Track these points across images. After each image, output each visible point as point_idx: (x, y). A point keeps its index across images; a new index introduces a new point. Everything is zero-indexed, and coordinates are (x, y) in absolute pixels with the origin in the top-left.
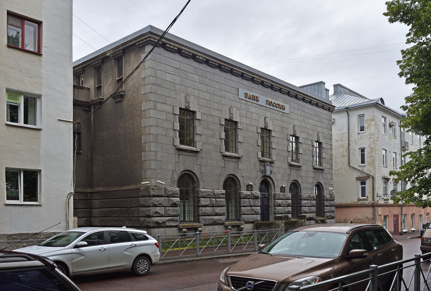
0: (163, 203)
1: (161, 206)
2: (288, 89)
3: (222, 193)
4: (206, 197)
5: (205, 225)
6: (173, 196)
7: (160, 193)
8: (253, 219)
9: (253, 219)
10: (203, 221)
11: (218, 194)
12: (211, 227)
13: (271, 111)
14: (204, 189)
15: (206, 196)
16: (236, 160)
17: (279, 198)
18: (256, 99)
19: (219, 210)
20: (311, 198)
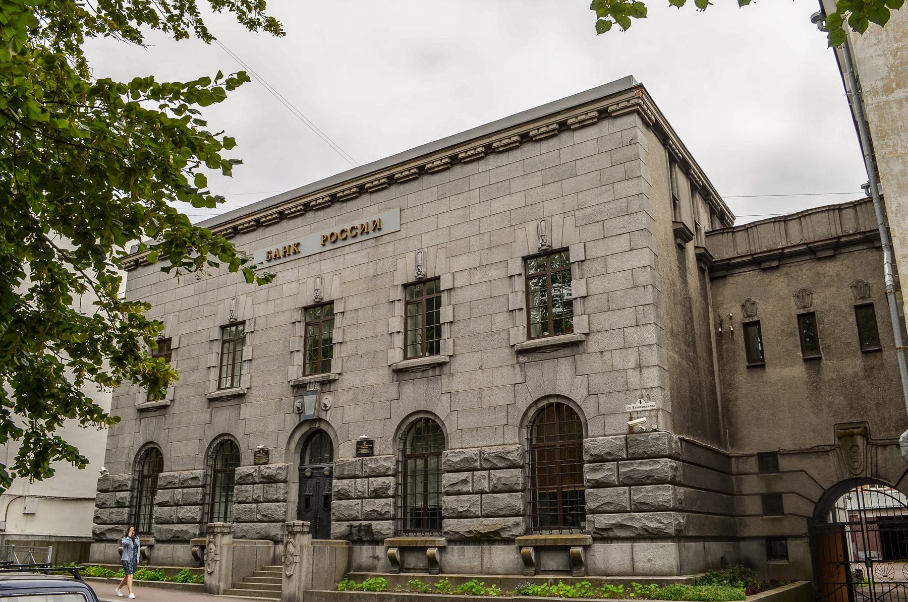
0: (107, 501)
1: (106, 506)
2: (382, 175)
3: (194, 476)
4: (167, 487)
5: (158, 541)
6: (120, 489)
7: (105, 485)
8: (258, 533)
9: (258, 533)
10: (158, 533)
11: (187, 480)
12: (169, 547)
13: (337, 254)
14: (171, 471)
15: (166, 485)
16: (236, 401)
17: (342, 476)
18: (292, 251)
19: (185, 512)
20: (487, 460)
